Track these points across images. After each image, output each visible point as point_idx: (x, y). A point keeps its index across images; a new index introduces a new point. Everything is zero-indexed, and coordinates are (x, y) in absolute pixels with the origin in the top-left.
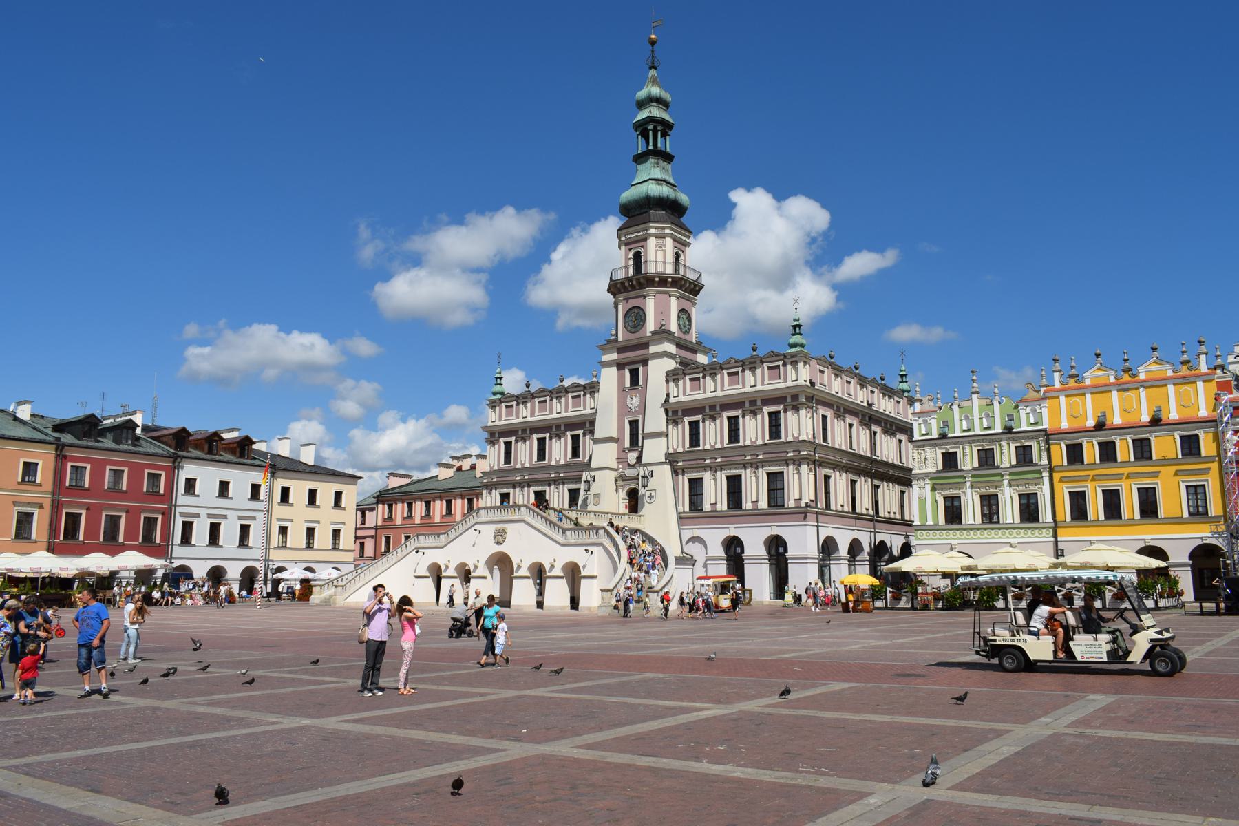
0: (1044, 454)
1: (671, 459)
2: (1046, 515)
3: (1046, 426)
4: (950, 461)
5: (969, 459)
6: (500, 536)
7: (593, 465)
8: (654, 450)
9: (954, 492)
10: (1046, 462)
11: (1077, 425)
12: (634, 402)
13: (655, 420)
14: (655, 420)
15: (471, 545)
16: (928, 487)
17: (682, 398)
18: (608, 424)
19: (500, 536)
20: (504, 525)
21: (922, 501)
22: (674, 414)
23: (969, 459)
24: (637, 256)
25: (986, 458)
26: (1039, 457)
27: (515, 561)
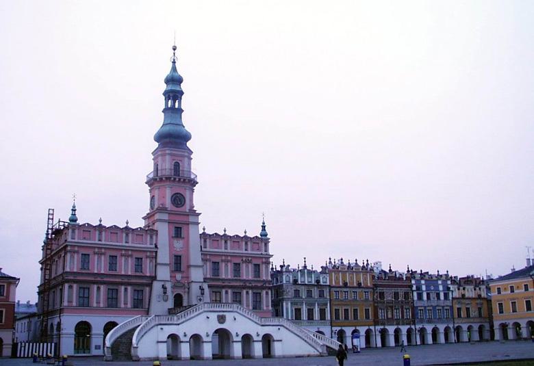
0: (328, 294)
1: (205, 280)
2: (328, 316)
3: (328, 284)
4: (297, 292)
5: (304, 295)
6: (222, 319)
7: (158, 279)
8: (197, 275)
9: (299, 307)
10: (328, 297)
11: (337, 285)
12: (178, 244)
13: (195, 257)
14: (195, 257)
15: (202, 323)
16: (289, 304)
17: (208, 249)
18: (164, 256)
19: (222, 319)
20: (224, 314)
21: (287, 309)
22: (204, 255)
23: (304, 295)
24: (177, 165)
25: (309, 293)
26: (326, 294)
27: (234, 334)
